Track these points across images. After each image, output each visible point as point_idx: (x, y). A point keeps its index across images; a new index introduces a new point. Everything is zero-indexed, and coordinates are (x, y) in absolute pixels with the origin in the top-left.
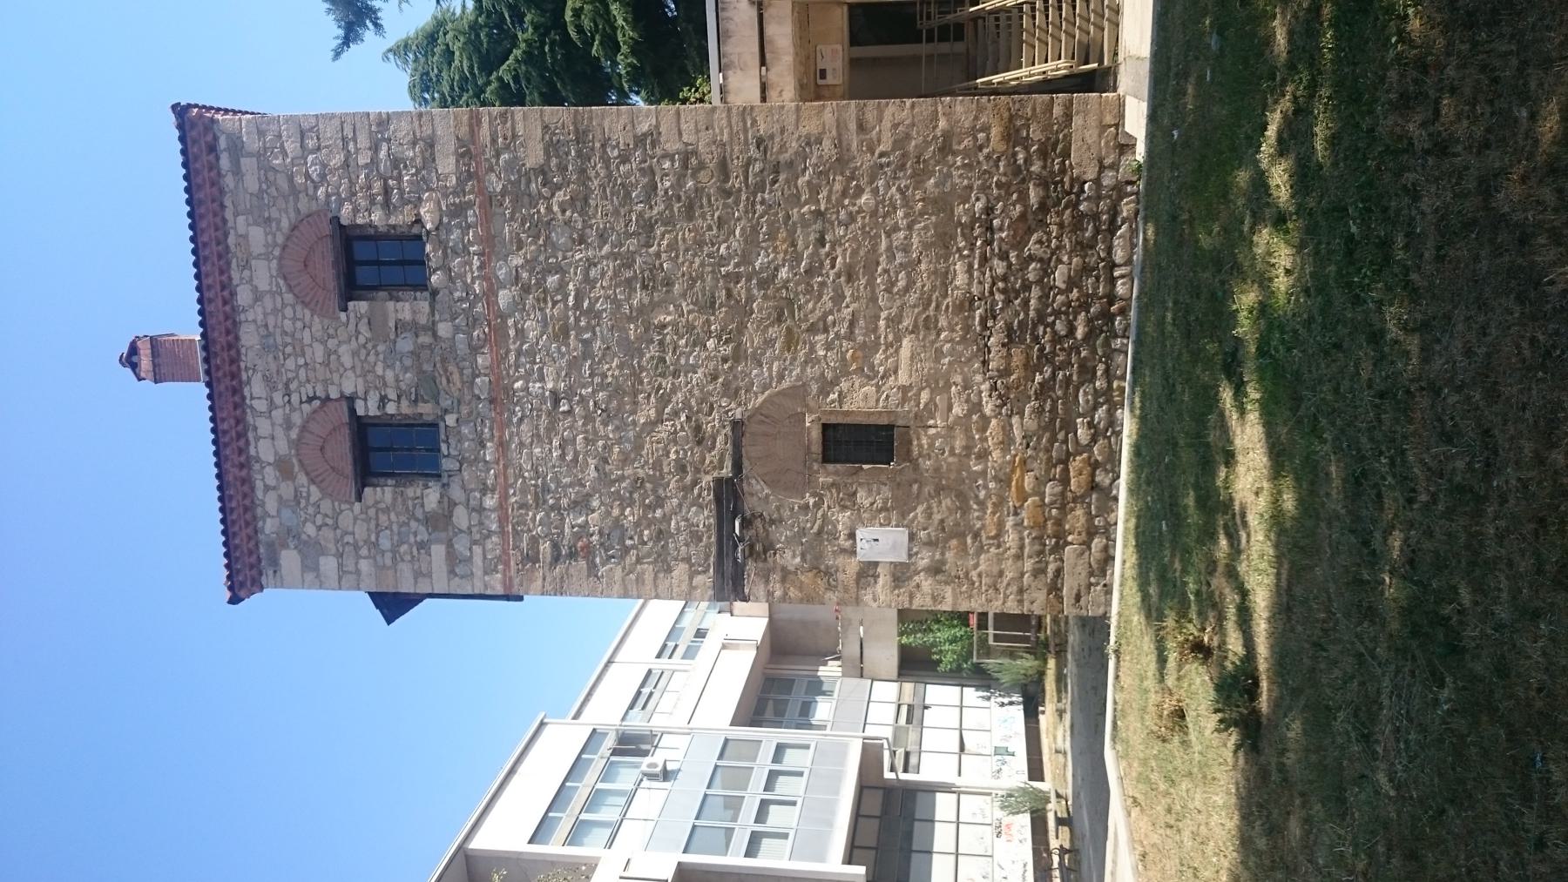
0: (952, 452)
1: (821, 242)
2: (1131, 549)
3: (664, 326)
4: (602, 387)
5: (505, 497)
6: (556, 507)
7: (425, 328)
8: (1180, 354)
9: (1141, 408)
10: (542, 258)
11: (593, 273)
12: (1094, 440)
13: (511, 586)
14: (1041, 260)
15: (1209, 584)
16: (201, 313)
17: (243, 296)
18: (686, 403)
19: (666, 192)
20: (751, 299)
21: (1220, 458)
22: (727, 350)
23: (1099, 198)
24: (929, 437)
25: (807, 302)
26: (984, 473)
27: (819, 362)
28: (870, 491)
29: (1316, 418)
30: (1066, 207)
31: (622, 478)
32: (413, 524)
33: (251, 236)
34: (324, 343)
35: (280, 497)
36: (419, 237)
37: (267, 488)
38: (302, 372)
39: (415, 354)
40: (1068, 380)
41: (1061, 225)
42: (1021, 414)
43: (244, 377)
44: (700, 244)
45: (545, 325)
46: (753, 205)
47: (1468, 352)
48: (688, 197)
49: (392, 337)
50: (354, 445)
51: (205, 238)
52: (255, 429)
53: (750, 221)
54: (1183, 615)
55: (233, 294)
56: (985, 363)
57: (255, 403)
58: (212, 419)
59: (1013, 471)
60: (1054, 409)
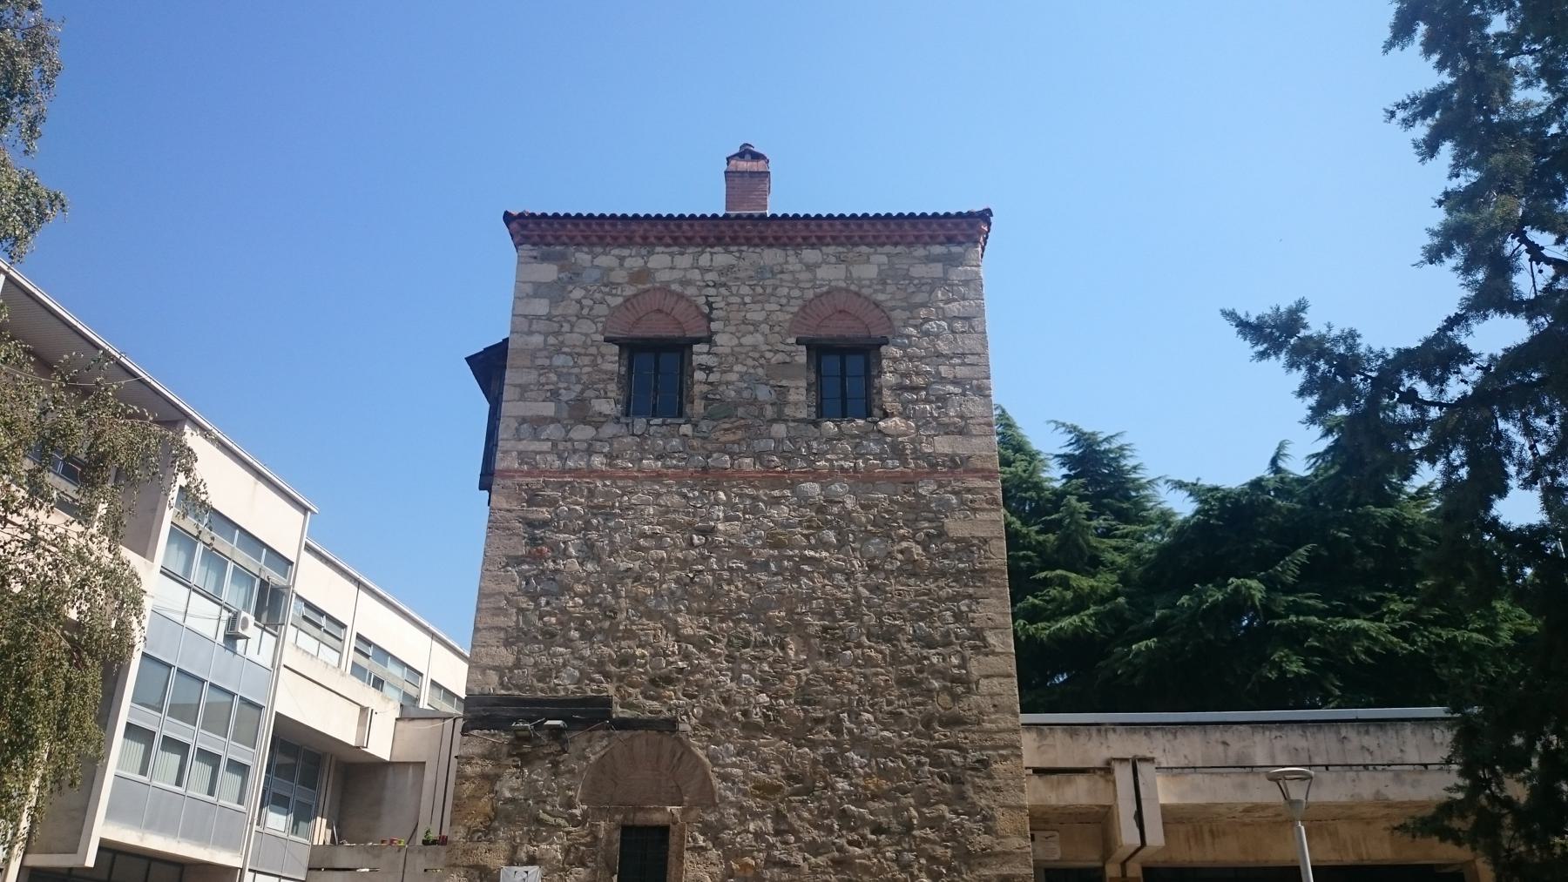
1: (878, 829)
3: (783, 648)
4: (718, 579)
5: (602, 476)
6: (588, 526)
10: (853, 527)
11: (839, 577)
13: (503, 477)
16: (796, 216)
17: (810, 255)
19: (926, 658)
20: (813, 745)
22: (757, 717)
27: (742, 823)
31: (617, 596)
32: (578, 388)
33: (869, 267)
34: (766, 321)
35: (612, 269)
37: (622, 259)
38: (738, 300)
43: (732, 248)
44: (873, 691)
46: (916, 753)
50: (661, 339)
51: (866, 226)
52: (682, 254)
53: (899, 747)
55: (813, 246)
58: (692, 217)
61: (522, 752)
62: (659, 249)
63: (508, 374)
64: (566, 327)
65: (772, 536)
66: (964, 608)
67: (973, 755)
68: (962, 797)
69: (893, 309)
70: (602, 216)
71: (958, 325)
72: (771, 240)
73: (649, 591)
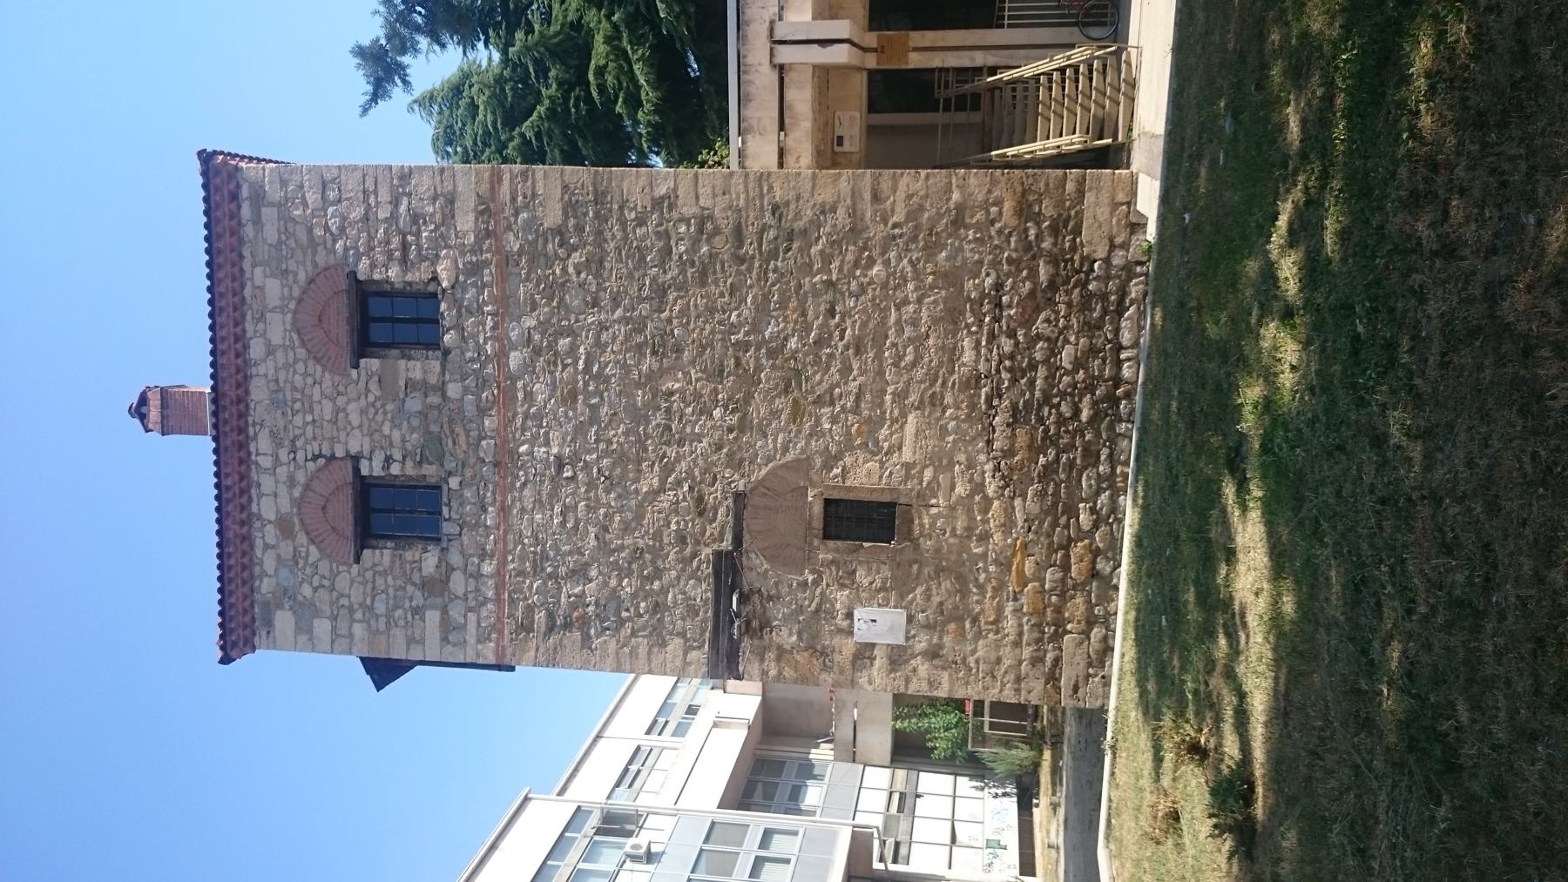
0: (953, 533)
1: (831, 313)
2: (1131, 642)
3: (672, 393)
4: (607, 453)
6: (553, 576)
7: (434, 388)
8: (1184, 445)
9: (1144, 498)
10: (554, 320)
11: (604, 337)
12: (1096, 526)
13: (504, 655)
14: (1048, 339)
15: (1207, 684)
16: (213, 365)
17: (256, 350)
18: (690, 473)
19: (681, 257)
20: (759, 368)
21: (1221, 555)
22: (733, 420)
23: (1108, 277)
24: (931, 516)
25: (815, 373)
26: (984, 556)
27: (824, 435)
28: (870, 569)
29: (1317, 521)
30: (1075, 287)
31: (622, 548)
32: (410, 589)
33: (267, 287)
34: (333, 400)
35: (279, 556)
36: (435, 295)
37: (267, 546)
38: (309, 429)
39: (423, 414)
40: (1071, 463)
41: (1069, 305)
42: (1024, 496)
43: (251, 431)
44: (712, 310)
45: (554, 389)
47: (1470, 464)
48: (702, 263)
49: (402, 396)
50: (355, 506)
51: (222, 289)
52: (259, 485)
53: (761, 289)
54: (1180, 714)
55: (246, 347)
56: (989, 442)
57: (260, 459)
58: (217, 475)
59: (1014, 555)
60: (1056, 493)
61: (758, 627)
62: (254, 508)
64: (344, 601)
65: (564, 401)
66: (633, 215)
67: (768, 218)
68: (805, 232)
69: (315, 265)
70: (220, 567)
71: (332, 195)
72: (240, 392)
73: (617, 518)
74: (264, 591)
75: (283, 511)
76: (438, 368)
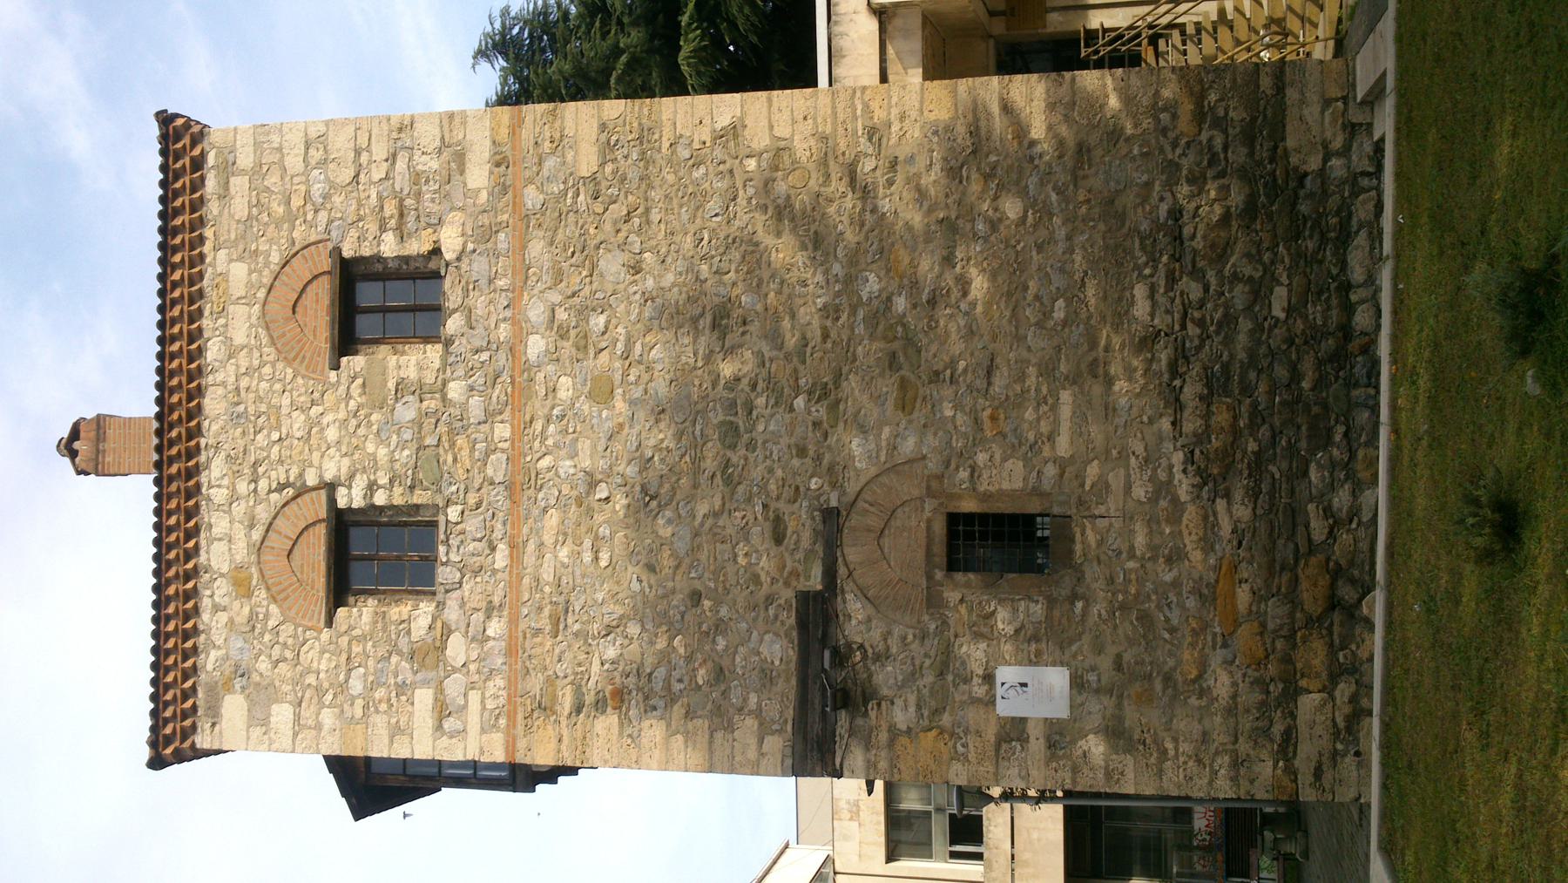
26: (1176, 584)
33: (230, 272)
37: (217, 608)
39: (418, 424)
42: (1227, 495)
52: (210, 526)
62: (203, 558)
63: (374, 754)
64: (311, 679)
74: (210, 667)
75: (238, 558)
76: (437, 364)
